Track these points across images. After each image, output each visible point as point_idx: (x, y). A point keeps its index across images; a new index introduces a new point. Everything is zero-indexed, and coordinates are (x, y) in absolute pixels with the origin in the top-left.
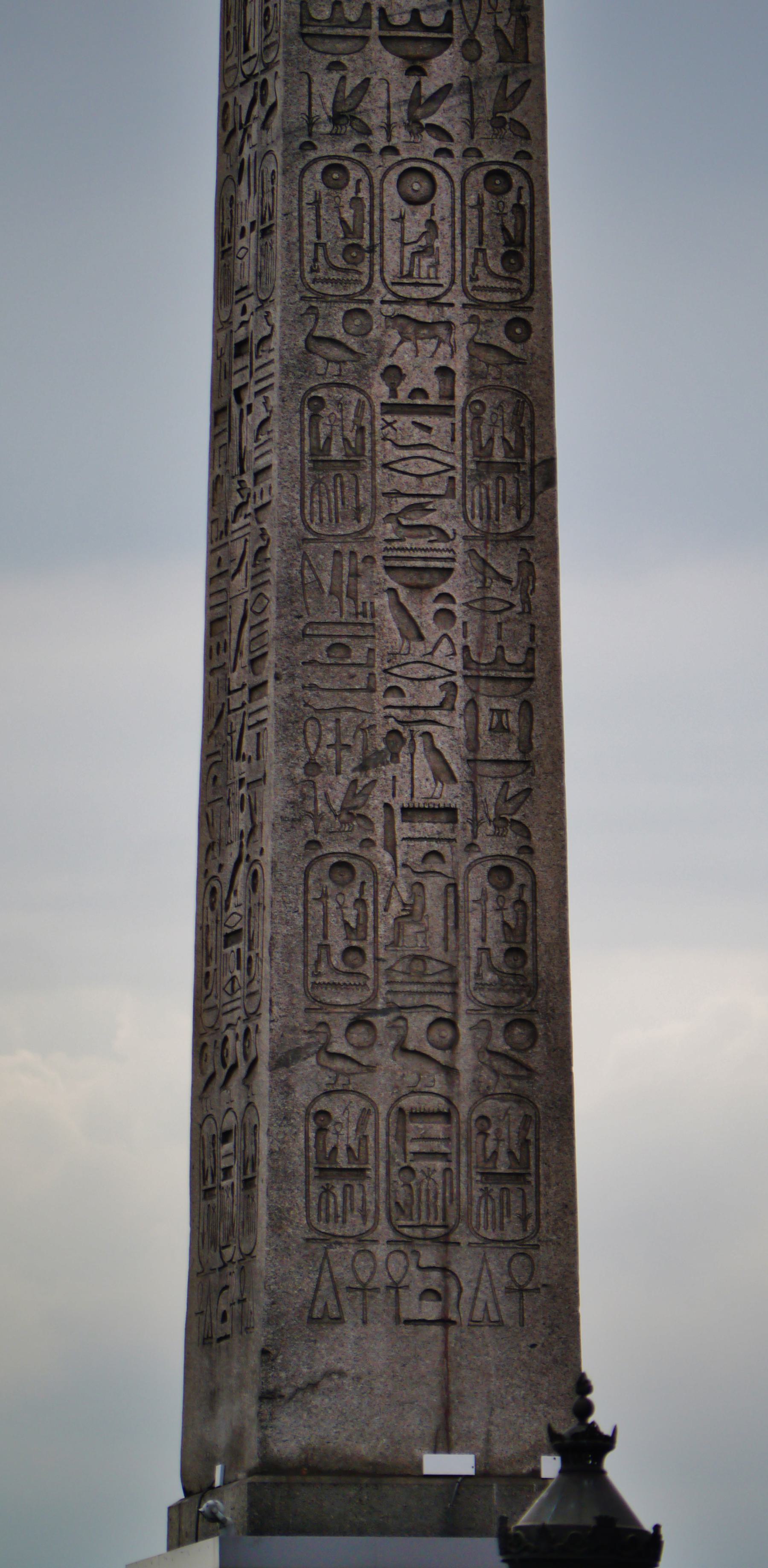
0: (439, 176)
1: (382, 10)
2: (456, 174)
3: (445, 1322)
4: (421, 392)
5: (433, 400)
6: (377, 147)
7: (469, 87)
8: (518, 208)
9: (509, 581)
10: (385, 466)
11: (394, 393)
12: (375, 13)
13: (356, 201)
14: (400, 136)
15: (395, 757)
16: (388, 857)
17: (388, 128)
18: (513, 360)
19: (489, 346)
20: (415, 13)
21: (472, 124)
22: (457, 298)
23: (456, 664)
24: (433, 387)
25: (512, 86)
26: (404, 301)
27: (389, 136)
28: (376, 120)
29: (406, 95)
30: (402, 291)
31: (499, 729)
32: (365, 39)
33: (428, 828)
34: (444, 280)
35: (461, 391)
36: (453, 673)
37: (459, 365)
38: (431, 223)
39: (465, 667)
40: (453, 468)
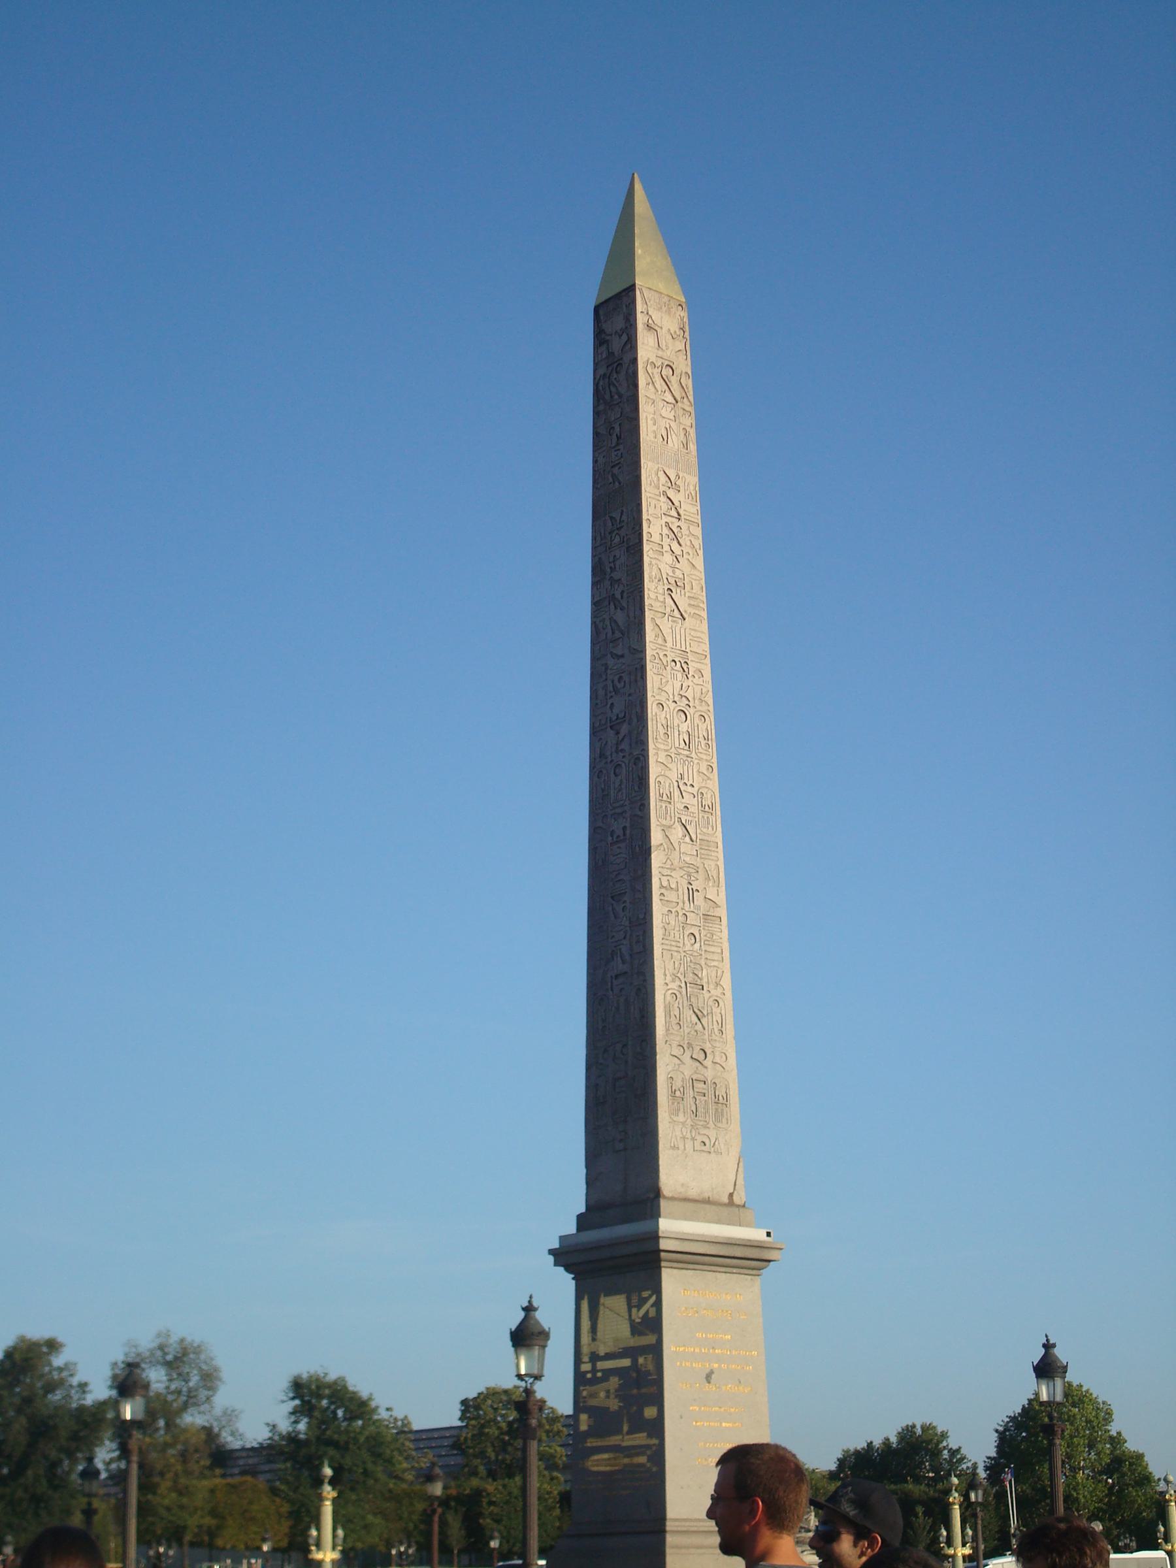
0: (623, 765)
1: (610, 718)
2: (627, 762)
3: (625, 1149)
4: (618, 836)
5: (622, 838)
6: (609, 761)
7: (630, 733)
8: (642, 767)
9: (640, 891)
10: (611, 863)
11: (613, 839)
12: (609, 719)
13: (605, 780)
14: (614, 755)
15: (613, 959)
16: (611, 992)
17: (611, 755)
18: (642, 817)
19: (635, 815)
20: (618, 715)
21: (630, 745)
22: (627, 803)
23: (627, 923)
24: (620, 833)
25: (641, 728)
26: (614, 808)
27: (611, 757)
28: (608, 753)
29: (614, 742)
30: (614, 805)
31: (638, 942)
32: (606, 728)
33: (621, 980)
34: (624, 798)
35: (628, 832)
36: (626, 926)
37: (628, 825)
38: (621, 781)
39: (630, 923)
40: (626, 858)
